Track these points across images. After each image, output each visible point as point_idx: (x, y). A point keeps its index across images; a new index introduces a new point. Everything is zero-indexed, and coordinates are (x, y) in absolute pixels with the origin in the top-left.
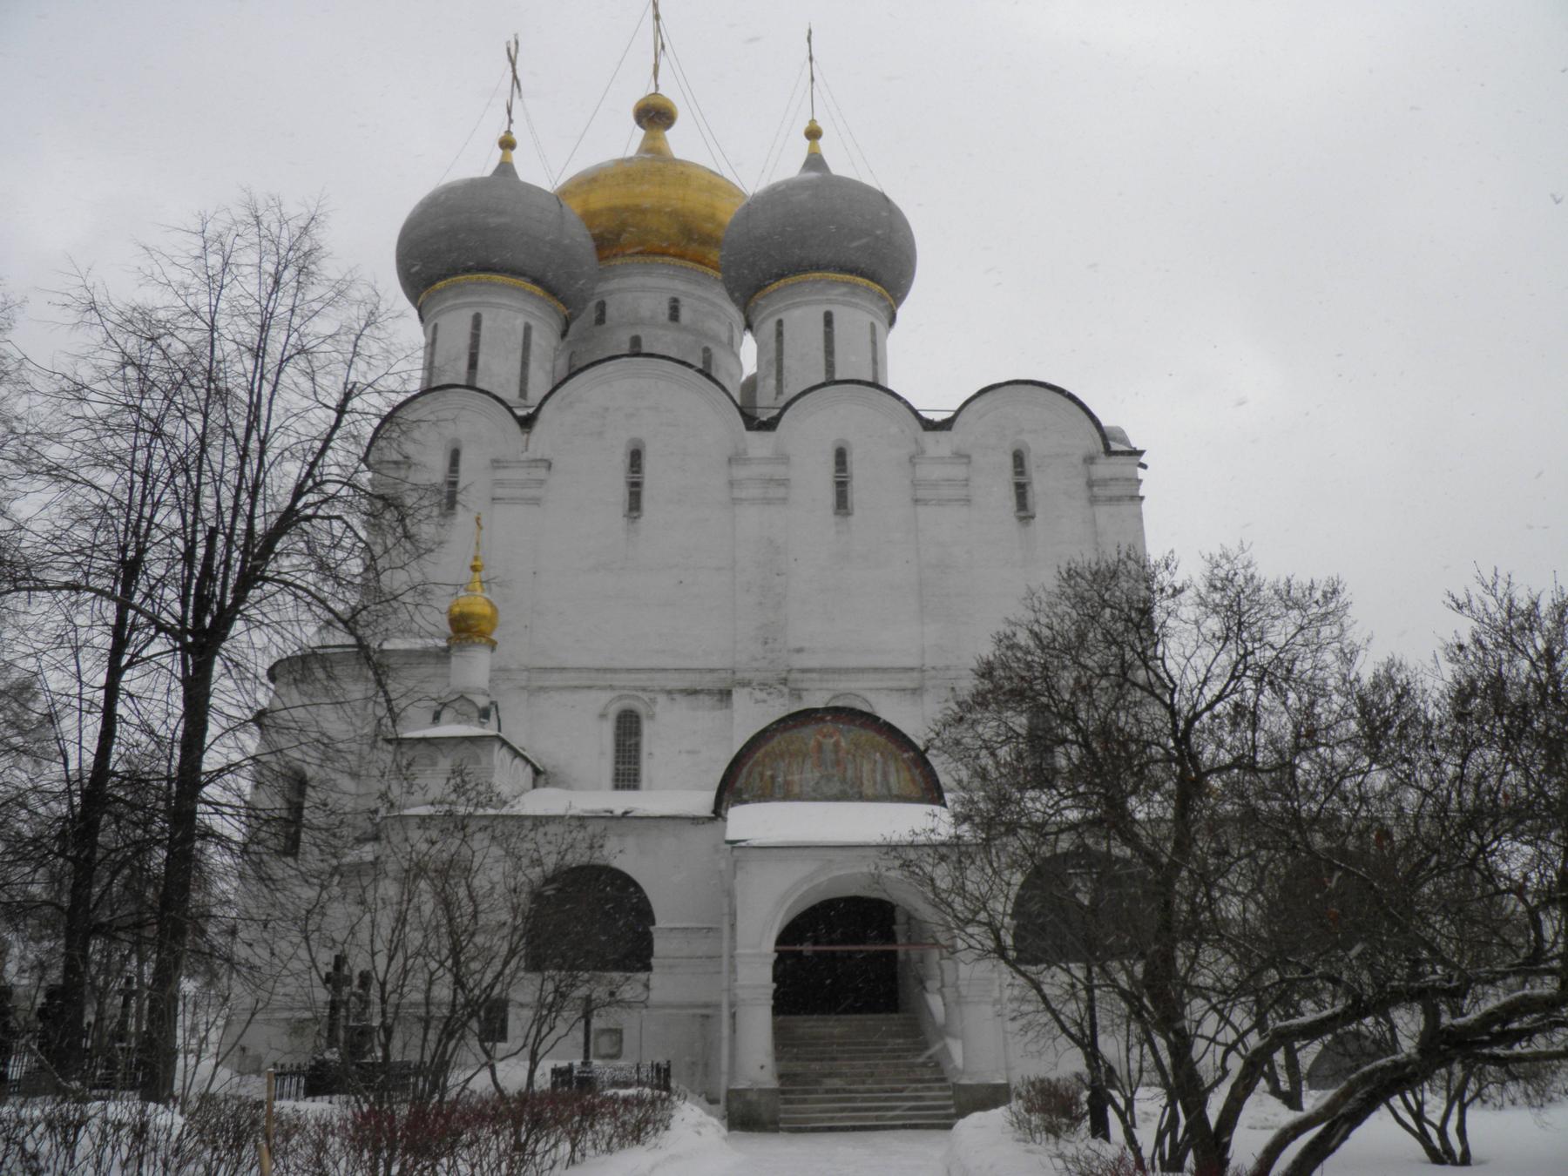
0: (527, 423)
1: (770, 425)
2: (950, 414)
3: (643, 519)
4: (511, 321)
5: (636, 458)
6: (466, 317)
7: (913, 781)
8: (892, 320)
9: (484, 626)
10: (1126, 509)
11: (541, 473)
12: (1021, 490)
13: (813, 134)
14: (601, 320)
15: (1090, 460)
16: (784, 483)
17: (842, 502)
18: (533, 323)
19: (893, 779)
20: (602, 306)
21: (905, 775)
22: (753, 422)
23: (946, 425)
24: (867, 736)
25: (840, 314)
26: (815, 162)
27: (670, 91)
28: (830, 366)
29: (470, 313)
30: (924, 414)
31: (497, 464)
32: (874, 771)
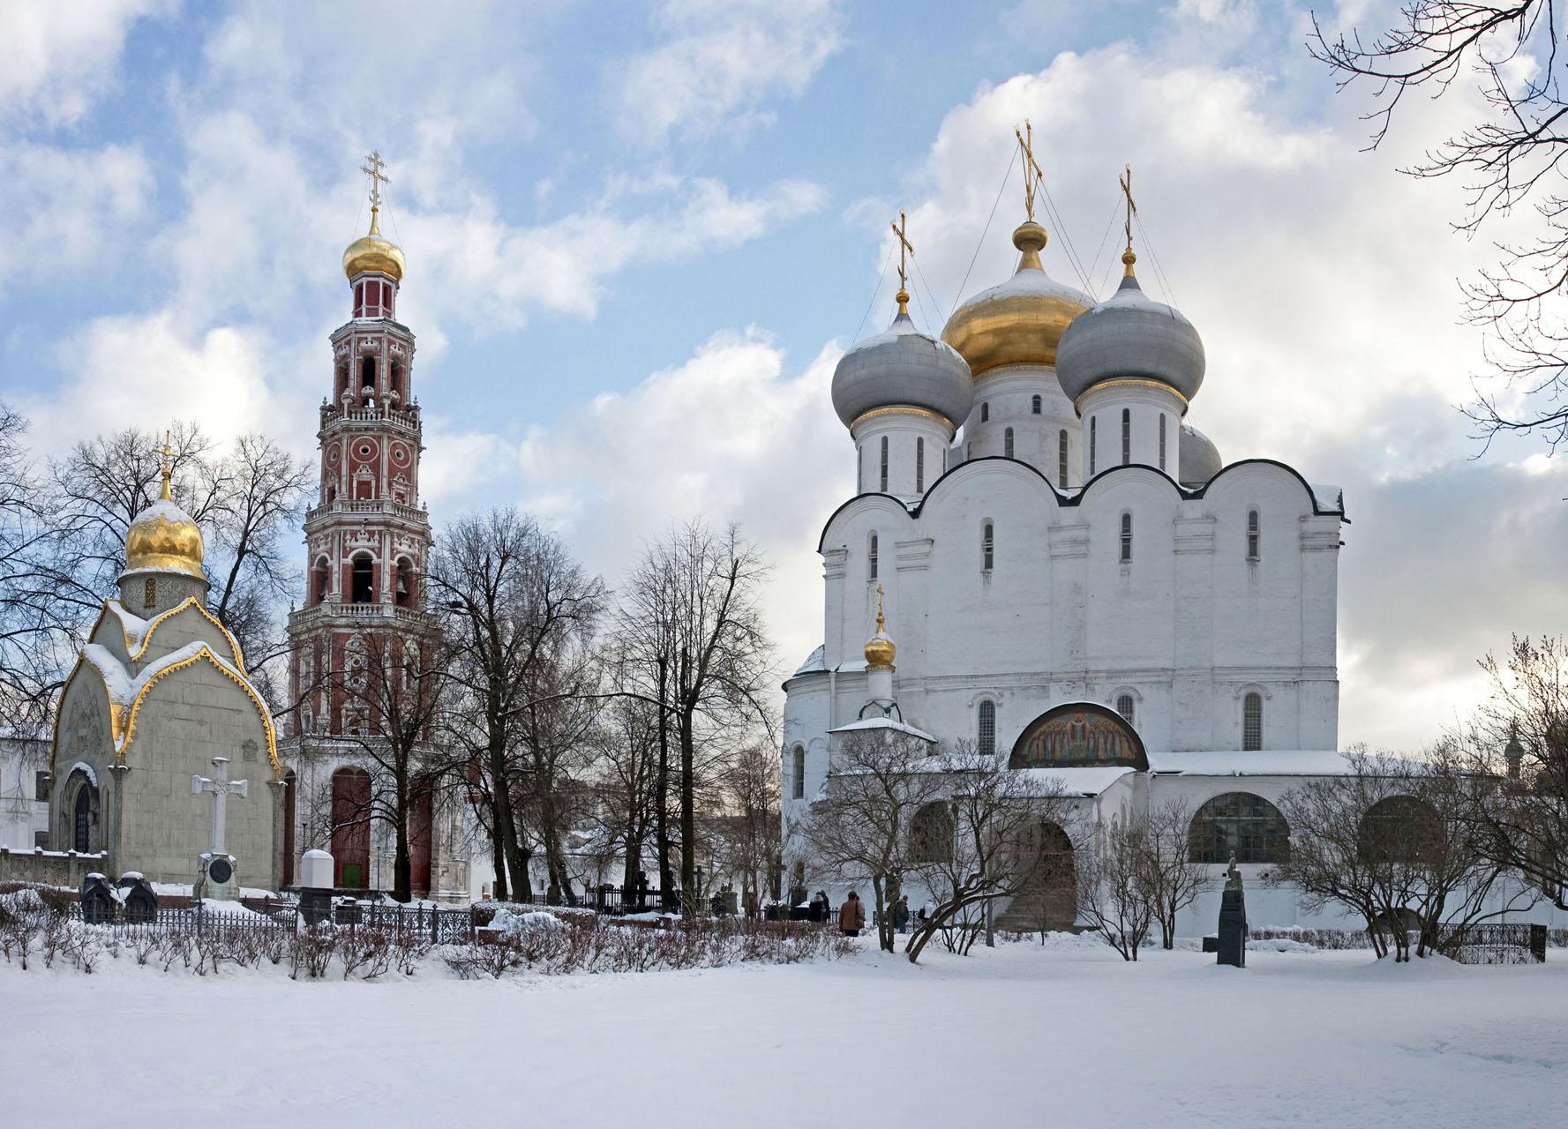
0: (915, 514)
1: (1075, 501)
5: (989, 530)
9: (887, 657)
11: (927, 548)
14: (985, 417)
16: (1087, 541)
17: (1126, 554)
19: (1117, 748)
20: (986, 407)
21: (1126, 745)
22: (1063, 501)
24: (1102, 720)
27: (1041, 220)
31: (898, 545)
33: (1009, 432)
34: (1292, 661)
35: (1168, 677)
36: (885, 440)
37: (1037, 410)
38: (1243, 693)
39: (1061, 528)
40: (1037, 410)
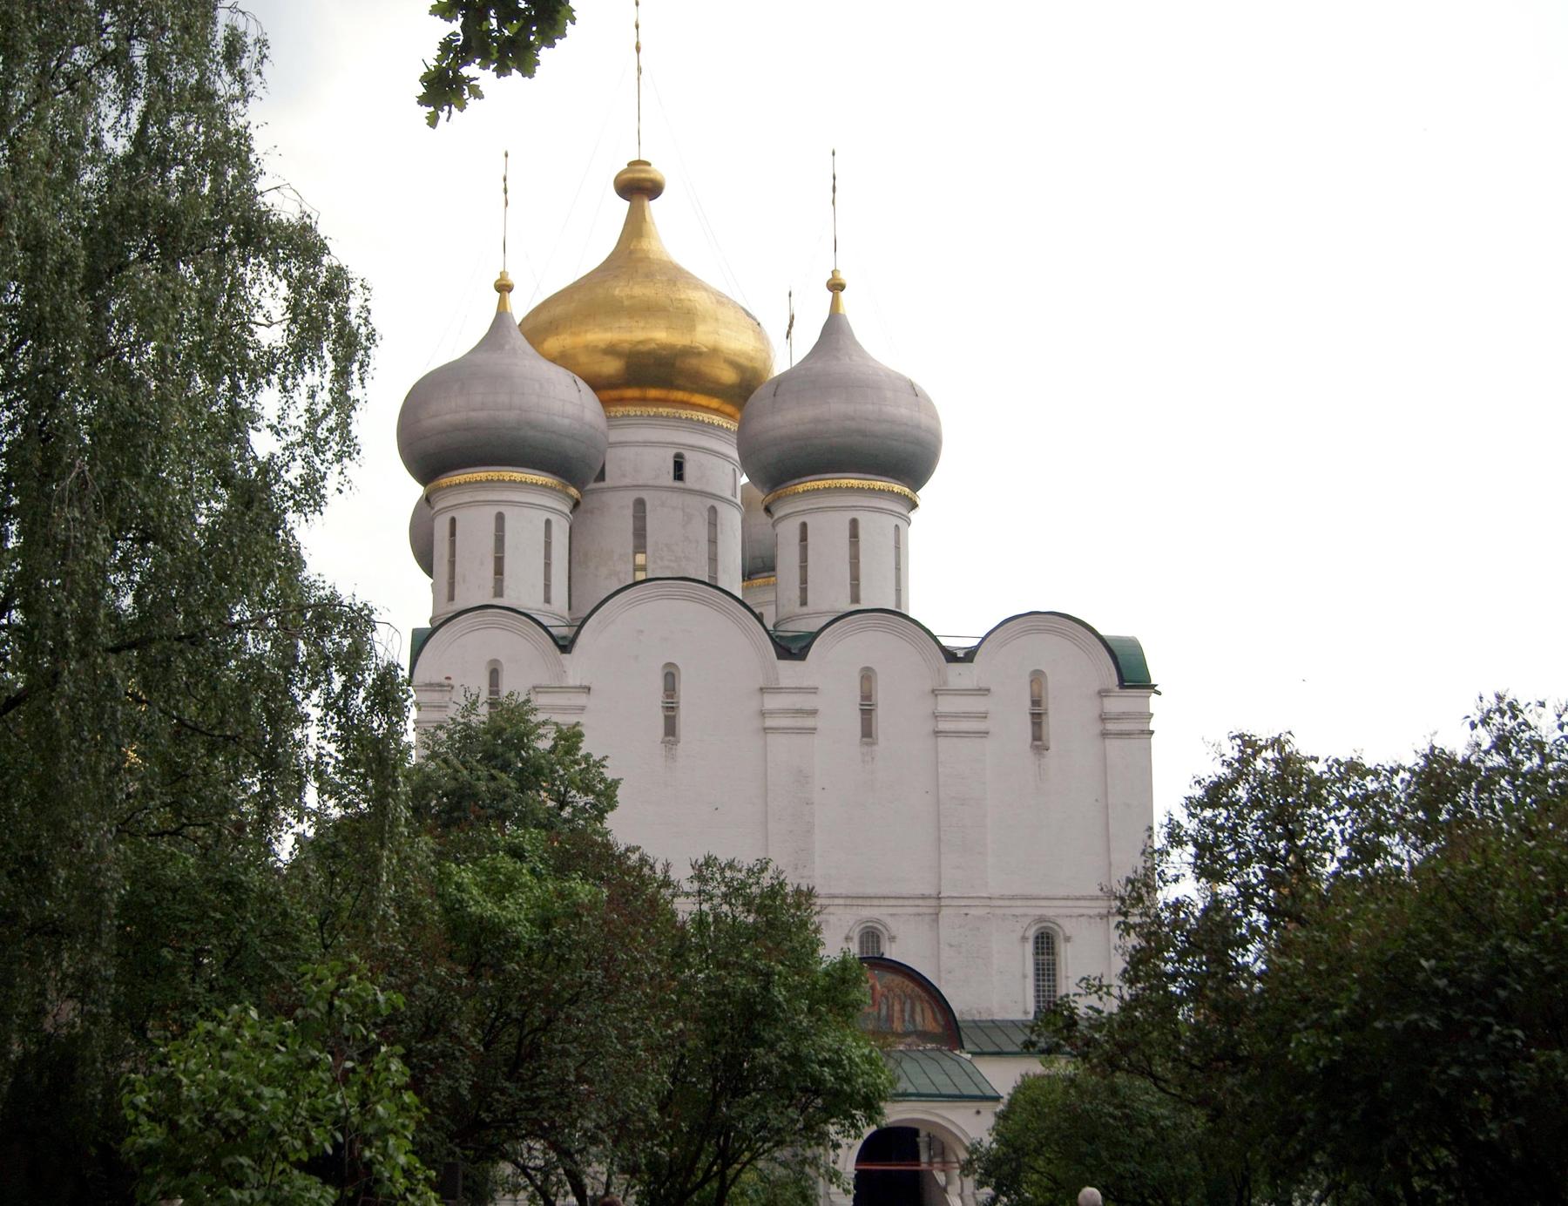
0: (565, 646)
1: (801, 655)
2: (975, 642)
3: (680, 746)
4: (530, 513)
6: (492, 511)
7: (935, 1019)
8: (914, 505)
10: (1134, 743)
12: (1037, 719)
13: (836, 286)
15: (1103, 693)
17: (867, 732)
18: (554, 518)
19: (918, 1018)
21: (928, 1014)
23: (970, 655)
25: (864, 518)
26: (834, 329)
28: (855, 598)
29: (494, 510)
30: (945, 642)
32: (902, 1011)
33: (640, 504)
36: (500, 518)
38: (1031, 933)
39: (778, 690)
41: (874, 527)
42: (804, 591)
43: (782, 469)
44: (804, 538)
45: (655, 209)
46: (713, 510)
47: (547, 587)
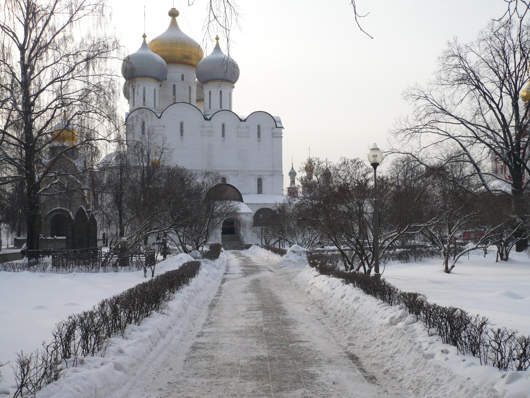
4: (150, 87)
8: (234, 87)
15: (273, 128)
16: (212, 132)
17: (223, 136)
22: (206, 119)
23: (245, 120)
28: (221, 107)
33: (174, 86)
34: (271, 169)
35: (237, 173)
37: (183, 79)
38: (257, 178)
40: (183, 79)
41: (225, 92)
42: (210, 106)
43: (205, 79)
44: (210, 94)
45: (177, 18)
46: (190, 87)
47: (155, 104)
